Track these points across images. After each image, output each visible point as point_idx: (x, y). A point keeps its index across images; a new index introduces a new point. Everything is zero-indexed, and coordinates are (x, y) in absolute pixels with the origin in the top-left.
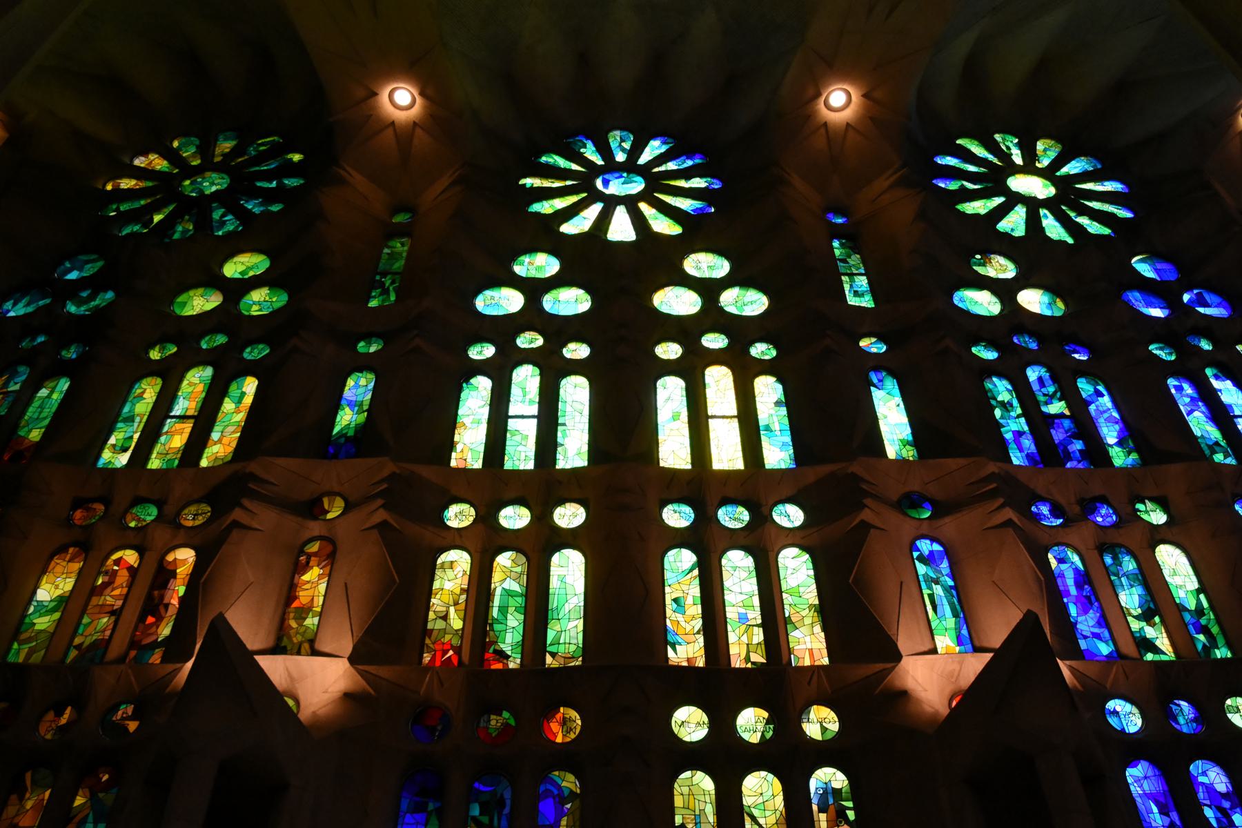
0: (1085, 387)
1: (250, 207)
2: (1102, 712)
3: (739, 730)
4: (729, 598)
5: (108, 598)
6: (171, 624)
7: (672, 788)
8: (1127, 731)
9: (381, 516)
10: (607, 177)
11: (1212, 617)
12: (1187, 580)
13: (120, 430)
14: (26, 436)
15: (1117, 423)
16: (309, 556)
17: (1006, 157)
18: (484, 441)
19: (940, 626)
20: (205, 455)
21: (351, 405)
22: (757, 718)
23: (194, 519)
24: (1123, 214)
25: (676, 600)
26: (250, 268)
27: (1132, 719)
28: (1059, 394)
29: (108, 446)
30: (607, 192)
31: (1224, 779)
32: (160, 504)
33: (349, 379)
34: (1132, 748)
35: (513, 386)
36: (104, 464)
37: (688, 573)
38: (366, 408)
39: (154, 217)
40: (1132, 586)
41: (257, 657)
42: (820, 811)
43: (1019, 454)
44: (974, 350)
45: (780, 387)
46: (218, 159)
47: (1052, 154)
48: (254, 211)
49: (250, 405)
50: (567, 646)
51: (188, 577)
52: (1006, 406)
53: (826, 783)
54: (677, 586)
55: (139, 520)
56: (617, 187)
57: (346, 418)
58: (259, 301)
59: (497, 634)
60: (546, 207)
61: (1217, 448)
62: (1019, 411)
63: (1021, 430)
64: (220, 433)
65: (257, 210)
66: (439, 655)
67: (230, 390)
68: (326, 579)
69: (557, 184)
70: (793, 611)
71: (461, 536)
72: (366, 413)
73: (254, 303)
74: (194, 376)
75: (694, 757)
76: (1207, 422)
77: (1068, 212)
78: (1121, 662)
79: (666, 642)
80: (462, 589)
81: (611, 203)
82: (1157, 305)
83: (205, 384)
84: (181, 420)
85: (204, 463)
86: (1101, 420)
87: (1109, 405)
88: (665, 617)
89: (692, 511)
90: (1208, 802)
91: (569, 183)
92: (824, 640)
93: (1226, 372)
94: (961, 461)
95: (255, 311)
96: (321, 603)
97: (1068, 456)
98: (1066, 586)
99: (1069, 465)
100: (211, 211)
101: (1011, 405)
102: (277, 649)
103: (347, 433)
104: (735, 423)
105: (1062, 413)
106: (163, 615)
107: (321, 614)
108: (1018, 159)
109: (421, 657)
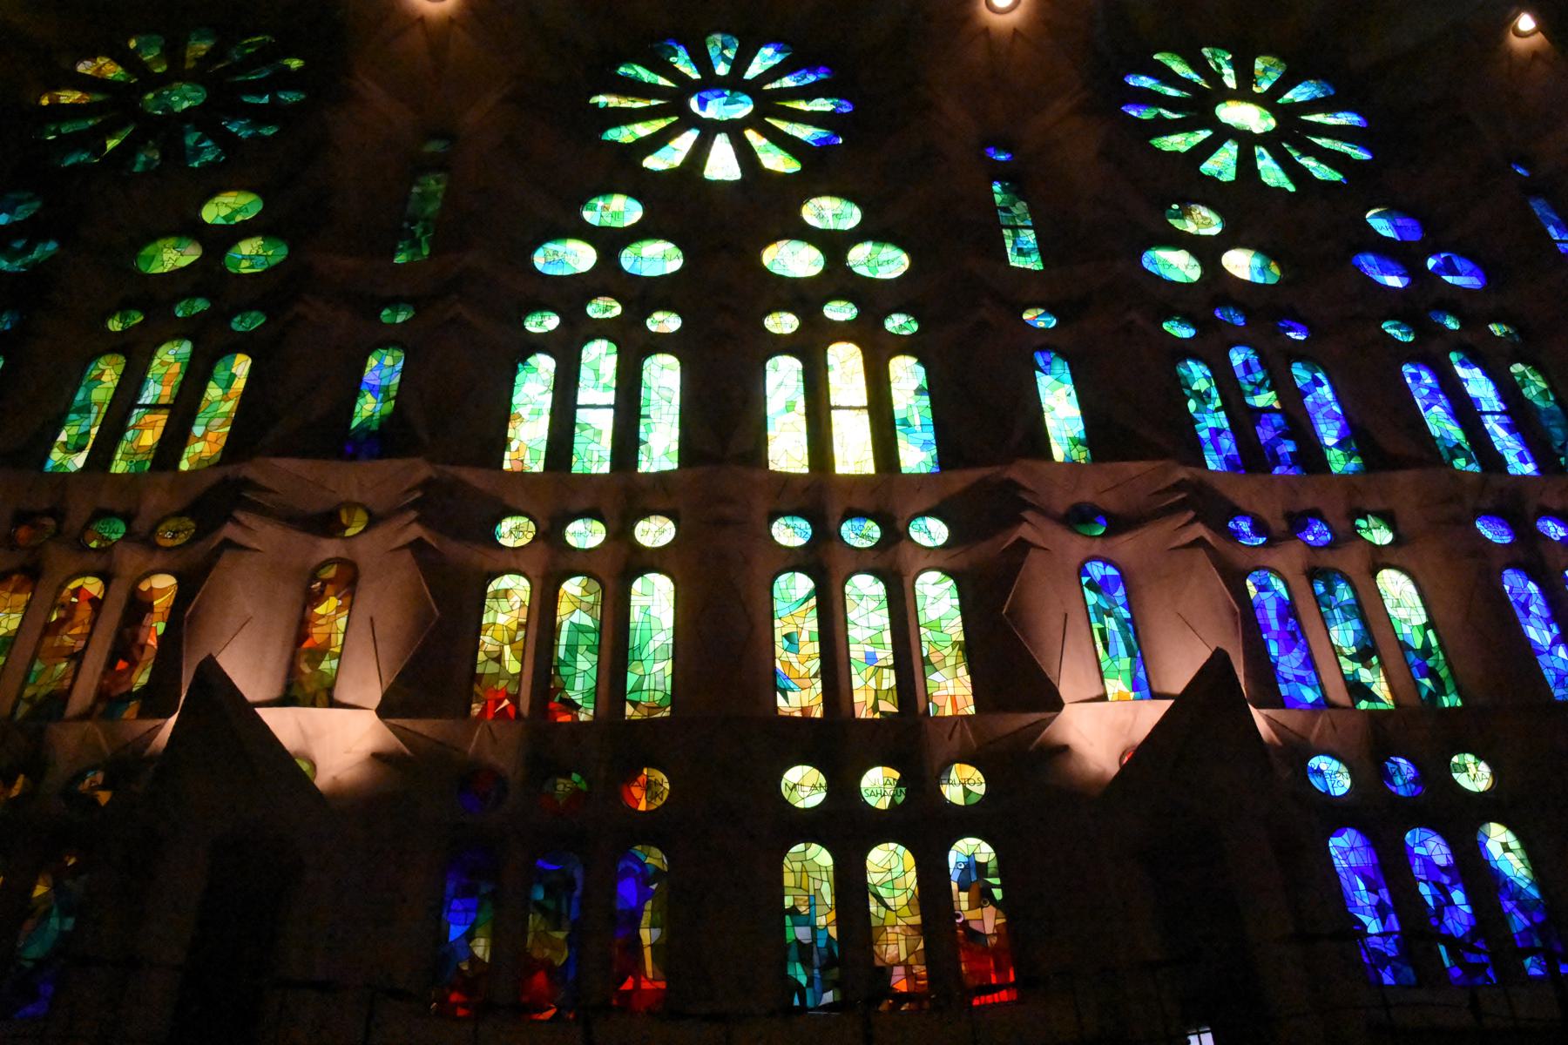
0: (1301, 374)
1: (235, 130)
2: (1303, 772)
3: (864, 794)
4: (853, 633)
5: (66, 638)
6: (149, 670)
7: (781, 863)
8: (1332, 794)
9: (416, 531)
10: (704, 95)
11: (1441, 657)
12: (1413, 612)
15: (1338, 419)
16: (325, 583)
17: (1215, 78)
18: (546, 438)
19: (1112, 668)
20: (185, 456)
21: (374, 390)
22: (885, 779)
23: (173, 537)
24: (1359, 154)
25: (787, 637)
26: (236, 211)
27: (1339, 779)
28: (1267, 383)
29: (58, 444)
30: (705, 115)
31: (1445, 850)
32: (128, 518)
33: (371, 357)
34: (1337, 814)
35: (582, 367)
36: (53, 467)
37: (803, 604)
38: (393, 393)
39: (107, 142)
40: (1347, 620)
41: (259, 710)
42: (961, 889)
43: (1216, 457)
44: (1166, 326)
45: (921, 370)
46: (190, 65)
47: (1274, 76)
48: (240, 135)
49: (241, 390)
50: (652, 693)
51: (169, 610)
52: (1202, 397)
53: (968, 857)
54: (789, 619)
55: (103, 539)
56: (717, 109)
57: (368, 407)
58: (250, 255)
59: (564, 679)
60: (625, 134)
61: (1458, 452)
62: (1218, 403)
63: (1219, 426)
64: (204, 428)
65: (244, 134)
67: (215, 371)
68: (347, 612)
69: (640, 104)
70: (932, 650)
72: (393, 402)
73: (244, 258)
74: (167, 353)
75: (809, 826)
76: (1448, 419)
77: (1291, 151)
78: (1330, 711)
79: (776, 688)
81: (709, 130)
82: (1394, 272)
83: (182, 363)
84: (153, 411)
85: (184, 466)
86: (1319, 416)
87: (1330, 397)
88: (774, 658)
89: (808, 526)
90: (1424, 877)
91: (654, 102)
92: (970, 685)
93: (1472, 359)
94: (1143, 466)
95: (245, 268)
96: (340, 642)
97: (1277, 460)
98: (1265, 618)
99: (1277, 470)
100: (183, 134)
101: (1209, 396)
102: (286, 699)
103: (370, 426)
104: (864, 417)
105: (1271, 407)
106: (138, 658)
108: (1230, 81)
109: (469, 709)
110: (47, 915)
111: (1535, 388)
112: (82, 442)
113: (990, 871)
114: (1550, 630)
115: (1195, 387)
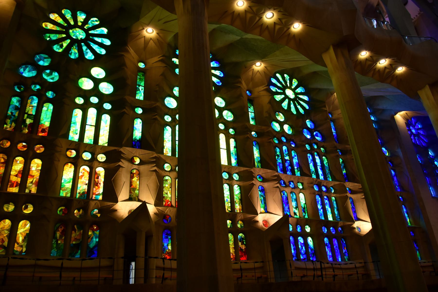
0: (293, 153)
5: (84, 180)
11: (306, 209)
13: (73, 127)
14: (44, 124)
24: (307, 107)
42: (240, 242)
43: (279, 168)
52: (278, 156)
61: (313, 172)
62: (280, 158)
66: (167, 203)
68: (139, 181)
71: (170, 174)
80: (170, 187)
93: (318, 155)
94: (271, 171)
96: (138, 187)
101: (279, 156)
104: (221, 147)
107: (139, 190)
109: (163, 203)
110: (92, 238)
111: (325, 162)
112: (77, 132)
113: (244, 239)
114: (321, 206)
115: (277, 154)
